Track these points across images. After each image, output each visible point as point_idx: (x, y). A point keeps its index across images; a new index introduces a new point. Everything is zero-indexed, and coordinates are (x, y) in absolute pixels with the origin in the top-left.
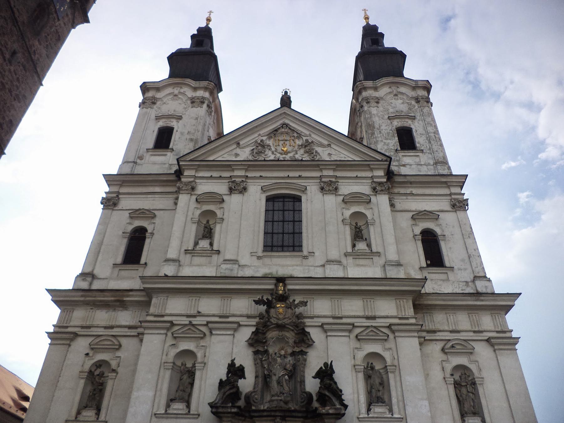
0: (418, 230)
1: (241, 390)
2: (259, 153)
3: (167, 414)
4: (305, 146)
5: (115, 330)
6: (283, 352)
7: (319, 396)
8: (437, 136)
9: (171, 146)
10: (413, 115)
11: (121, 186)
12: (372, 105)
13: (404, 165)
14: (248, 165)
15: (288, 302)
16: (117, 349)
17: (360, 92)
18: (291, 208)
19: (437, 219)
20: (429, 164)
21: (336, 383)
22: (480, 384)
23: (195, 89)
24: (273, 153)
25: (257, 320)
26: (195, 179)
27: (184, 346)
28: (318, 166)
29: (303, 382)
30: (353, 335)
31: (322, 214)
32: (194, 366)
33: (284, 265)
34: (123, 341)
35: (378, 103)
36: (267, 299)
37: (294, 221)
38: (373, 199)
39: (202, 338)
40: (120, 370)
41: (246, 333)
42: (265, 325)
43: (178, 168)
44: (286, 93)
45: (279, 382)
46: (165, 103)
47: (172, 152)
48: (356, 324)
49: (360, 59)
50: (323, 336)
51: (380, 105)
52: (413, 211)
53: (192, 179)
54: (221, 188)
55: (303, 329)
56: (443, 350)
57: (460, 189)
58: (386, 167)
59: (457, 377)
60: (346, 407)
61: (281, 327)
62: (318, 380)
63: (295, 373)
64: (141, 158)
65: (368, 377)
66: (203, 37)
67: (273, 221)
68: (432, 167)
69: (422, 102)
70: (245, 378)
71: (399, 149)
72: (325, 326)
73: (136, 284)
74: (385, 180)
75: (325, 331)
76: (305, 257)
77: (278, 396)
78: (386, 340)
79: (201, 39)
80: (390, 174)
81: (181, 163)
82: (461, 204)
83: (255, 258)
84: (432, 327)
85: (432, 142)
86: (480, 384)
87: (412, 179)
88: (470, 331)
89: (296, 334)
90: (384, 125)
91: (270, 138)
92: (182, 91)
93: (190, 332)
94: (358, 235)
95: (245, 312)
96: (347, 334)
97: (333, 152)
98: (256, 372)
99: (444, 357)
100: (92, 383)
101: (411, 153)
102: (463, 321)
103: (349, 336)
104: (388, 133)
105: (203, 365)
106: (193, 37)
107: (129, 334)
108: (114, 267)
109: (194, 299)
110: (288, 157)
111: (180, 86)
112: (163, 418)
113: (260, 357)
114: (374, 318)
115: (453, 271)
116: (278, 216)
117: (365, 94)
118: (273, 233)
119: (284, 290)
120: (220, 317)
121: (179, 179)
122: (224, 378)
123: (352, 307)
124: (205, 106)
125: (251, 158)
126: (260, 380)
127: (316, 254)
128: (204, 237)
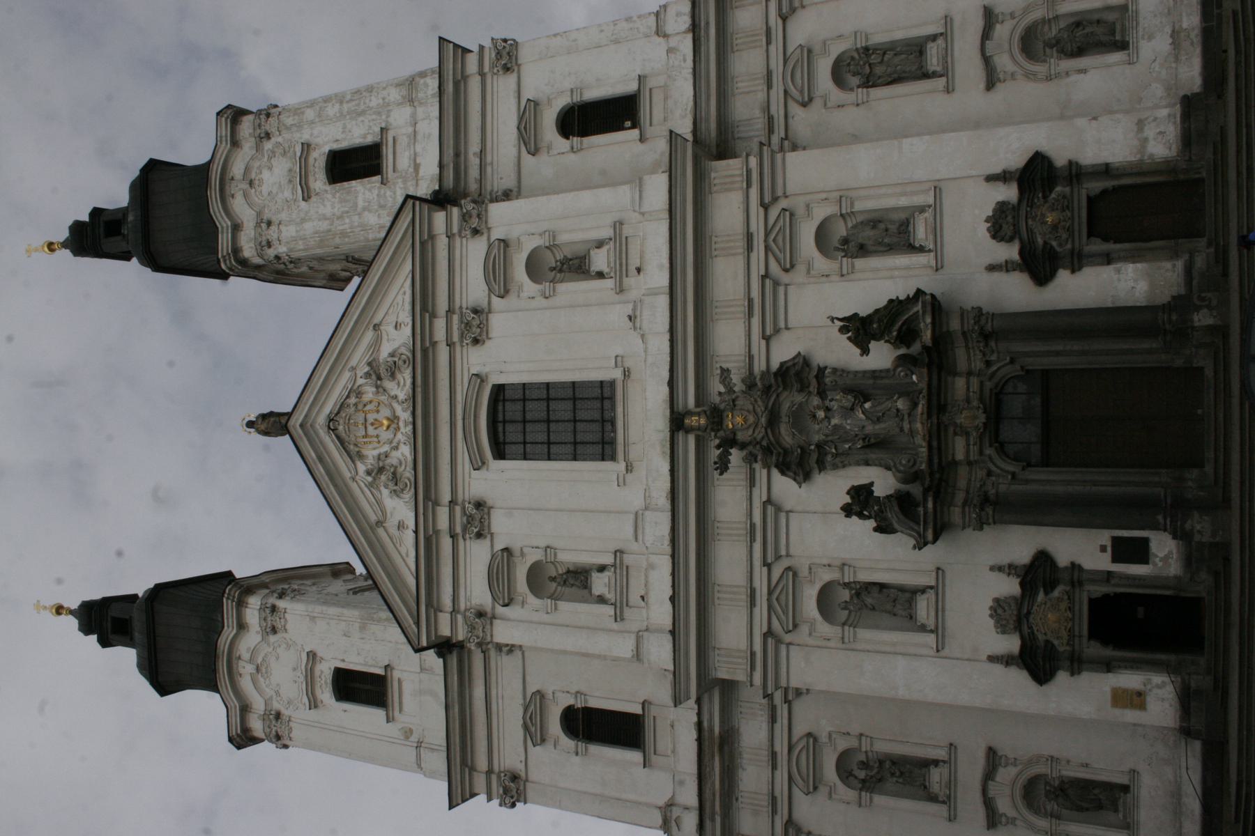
0: (562, 144)
1: (891, 492)
2: (395, 478)
3: (938, 630)
4: (379, 378)
5: (778, 748)
6: (821, 414)
7: (901, 342)
8: (348, 97)
9: (381, 672)
10: (298, 149)
11: (472, 769)
12: (275, 236)
13: (417, 167)
14: (426, 498)
15: (722, 406)
16: (815, 740)
17: (244, 262)
18: (519, 406)
19: (536, 104)
20: (414, 115)
21: (877, 311)
22: (867, 39)
23: (242, 626)
24: (396, 448)
25: (757, 466)
26: (458, 612)
28: (425, 351)
29: (875, 374)
30: (785, 278)
31: (531, 342)
32: (847, 585)
33: (645, 416)
34: (799, 730)
35: (269, 223)
36: (718, 447)
37: (548, 399)
38: (497, 234)
39: (795, 575)
40: (855, 729)
41: (784, 486)
42: (768, 451)
43: (431, 652)
44: (250, 424)
45: (879, 420)
46: (277, 693)
47: (392, 669)
48: (762, 272)
49: (156, 263)
50: (785, 335)
51: (274, 219)
52: (519, 152)
53: (460, 617)
54: (477, 556)
55: (776, 374)
56: (804, 105)
57: (469, 56)
58: (426, 207)
59: (855, 81)
60: (919, 292)
61: (773, 420)
62: (873, 345)
63: (860, 389)
64: (408, 733)
65: (863, 250)
66: (104, 620)
67: (549, 443)
68: (420, 110)
69: (267, 128)
70: (872, 484)
71: (378, 178)
72: (768, 333)
73: (686, 716)
74: (455, 210)
75: (777, 331)
76: (627, 373)
77: (902, 420)
78: (792, 215)
79: (109, 625)
80: (441, 199)
81: (424, 644)
82: (504, 53)
83: (629, 477)
84: (760, 124)
85: (362, 107)
86: (867, 39)
87: (450, 152)
88: (767, 51)
89: (785, 389)
90: (322, 210)
91: (361, 456)
92: (246, 656)
93: (783, 598)
94: (576, 266)
95: (742, 492)
96: (781, 290)
97: (392, 319)
98: (858, 464)
99: (817, 103)
100: (880, 780)
101: (387, 153)
102: (748, 64)
103: (786, 285)
104: (342, 201)
105: (846, 568)
106: (105, 643)
107: (786, 722)
108: (650, 766)
109: (717, 595)
110: (405, 416)
111: (234, 661)
112: (943, 636)
113: (829, 458)
114: (749, 237)
115: (645, 77)
116: (537, 433)
117: (248, 252)
118: (575, 443)
119: (699, 414)
120: (752, 540)
121: (461, 646)
122: (872, 523)
123: (729, 278)
124: (281, 604)
125: (408, 495)
126: (872, 456)
127: (620, 351)
128: (586, 585)
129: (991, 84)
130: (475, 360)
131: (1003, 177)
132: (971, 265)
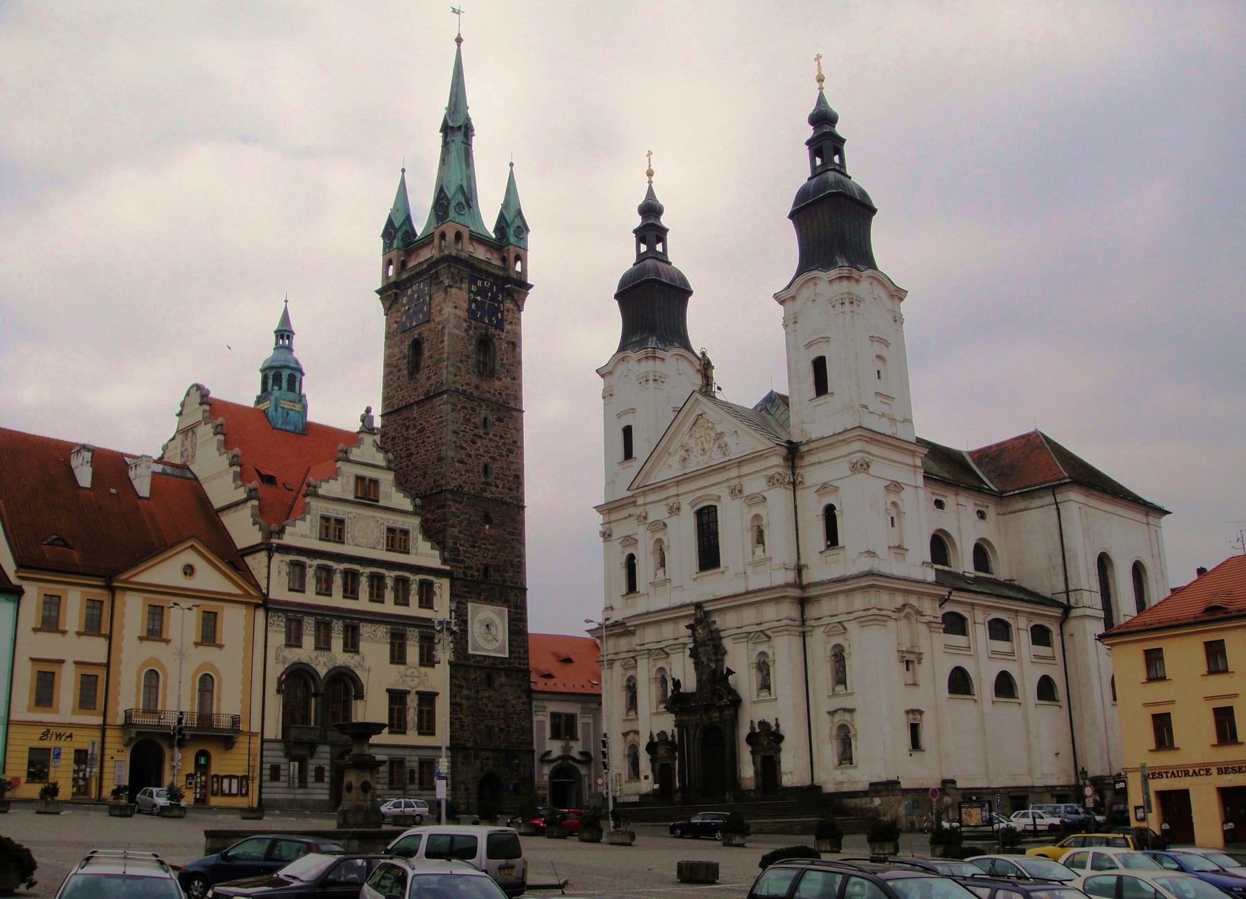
0: (820, 510)
3: (657, 714)
14: (678, 481)
27: (660, 664)
61: (703, 644)
102: (841, 604)
123: (749, 617)
129: (829, 713)
130: (724, 492)
131: (777, 725)
132: (753, 712)
